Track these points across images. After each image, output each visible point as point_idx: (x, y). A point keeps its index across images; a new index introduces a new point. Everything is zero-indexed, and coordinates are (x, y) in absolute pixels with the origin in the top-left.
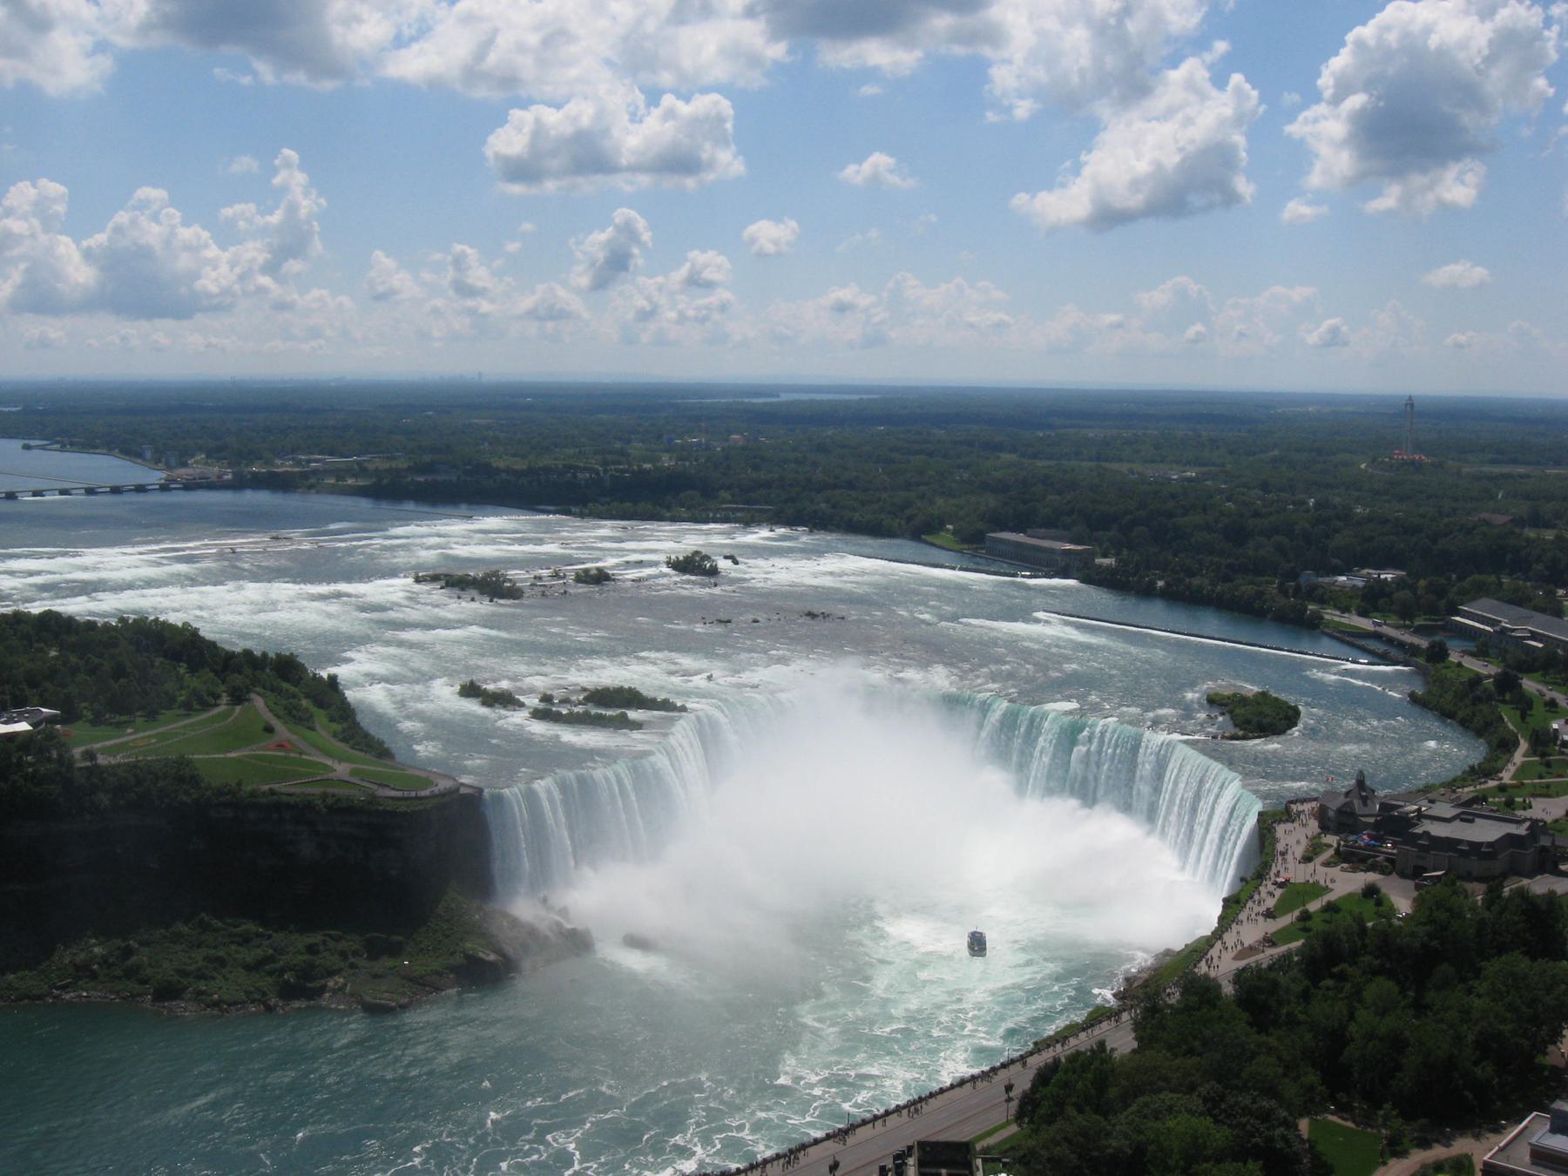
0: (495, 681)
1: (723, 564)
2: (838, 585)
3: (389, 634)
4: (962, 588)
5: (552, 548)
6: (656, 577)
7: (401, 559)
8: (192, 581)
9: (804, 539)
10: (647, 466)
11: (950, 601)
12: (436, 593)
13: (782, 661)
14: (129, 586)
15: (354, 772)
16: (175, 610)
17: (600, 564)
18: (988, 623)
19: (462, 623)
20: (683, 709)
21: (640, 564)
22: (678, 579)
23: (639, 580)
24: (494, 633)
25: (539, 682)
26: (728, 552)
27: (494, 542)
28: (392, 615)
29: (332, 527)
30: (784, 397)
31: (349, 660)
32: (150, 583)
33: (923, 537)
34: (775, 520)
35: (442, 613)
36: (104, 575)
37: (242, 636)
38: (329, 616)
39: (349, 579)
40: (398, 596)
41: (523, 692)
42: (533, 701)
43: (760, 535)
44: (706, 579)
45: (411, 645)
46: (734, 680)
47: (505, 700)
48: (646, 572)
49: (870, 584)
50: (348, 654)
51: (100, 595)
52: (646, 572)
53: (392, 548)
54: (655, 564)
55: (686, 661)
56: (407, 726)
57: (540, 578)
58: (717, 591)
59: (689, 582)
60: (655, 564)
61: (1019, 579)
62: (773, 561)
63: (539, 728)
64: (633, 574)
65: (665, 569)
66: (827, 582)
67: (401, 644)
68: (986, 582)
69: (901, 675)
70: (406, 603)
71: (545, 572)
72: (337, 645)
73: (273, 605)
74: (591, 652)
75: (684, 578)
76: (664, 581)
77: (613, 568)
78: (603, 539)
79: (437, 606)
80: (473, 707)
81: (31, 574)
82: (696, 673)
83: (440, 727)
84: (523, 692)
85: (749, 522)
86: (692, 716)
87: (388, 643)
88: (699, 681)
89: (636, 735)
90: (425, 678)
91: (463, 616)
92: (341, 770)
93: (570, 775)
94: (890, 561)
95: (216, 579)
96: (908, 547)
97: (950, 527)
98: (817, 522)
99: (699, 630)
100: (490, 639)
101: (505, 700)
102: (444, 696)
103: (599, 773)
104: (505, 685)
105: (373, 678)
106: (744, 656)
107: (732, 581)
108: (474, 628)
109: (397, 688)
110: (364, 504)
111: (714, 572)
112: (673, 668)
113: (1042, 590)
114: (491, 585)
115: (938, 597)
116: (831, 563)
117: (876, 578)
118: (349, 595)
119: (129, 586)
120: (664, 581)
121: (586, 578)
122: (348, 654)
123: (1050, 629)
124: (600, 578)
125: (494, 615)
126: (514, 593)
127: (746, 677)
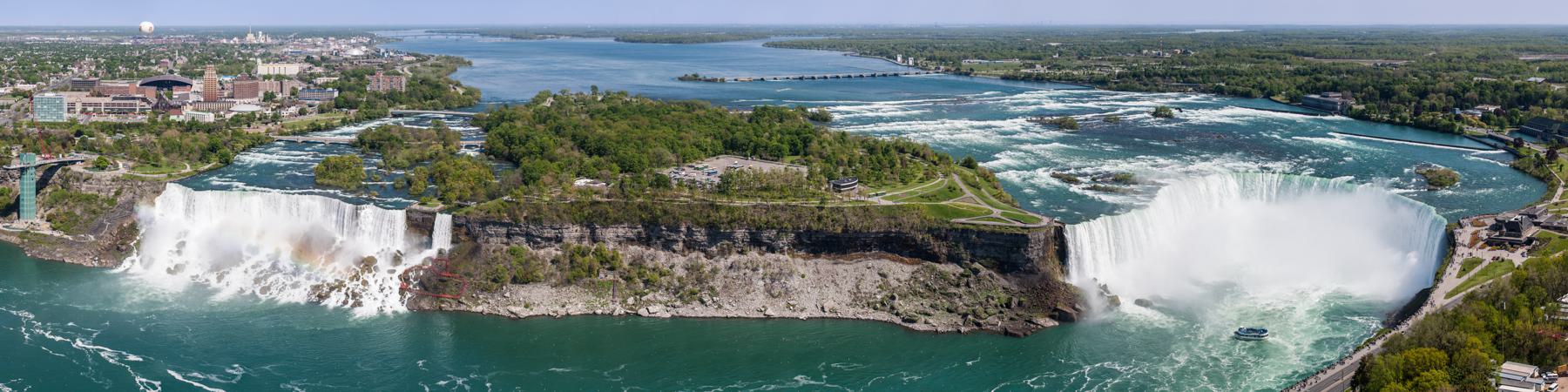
0: (1068, 170)
1: (1175, 112)
2: (1233, 122)
3: (1015, 146)
4: (1293, 122)
5: (1091, 105)
6: (1142, 119)
7: (1020, 109)
8: (922, 118)
9: (1215, 99)
10: (1135, 65)
11: (1286, 129)
12: (1038, 128)
13: (1206, 159)
14: (892, 119)
15: (1003, 214)
16: (916, 132)
17: (1116, 112)
18: (1309, 139)
19: (1051, 142)
20: (1162, 184)
21: (1135, 112)
22: (1153, 119)
23: (1135, 121)
24: (1065, 146)
25: (1089, 170)
26: (1177, 106)
27: (1063, 102)
28: (1015, 137)
29: (986, 93)
30: (1198, 31)
31: (997, 159)
32: (903, 119)
33: (1272, 98)
34: (1198, 90)
35: (1039, 136)
36: (880, 114)
37: (947, 145)
38: (986, 136)
39: (995, 119)
40: (1018, 128)
41: (1080, 175)
42: (1088, 179)
43: (1192, 98)
44: (1167, 119)
45: (1026, 152)
46: (1185, 170)
47: (1071, 180)
48: (1138, 116)
49: (1248, 121)
50: (997, 155)
51: (880, 124)
52: (1138, 116)
53: (1015, 105)
54: (1142, 112)
55: (1161, 161)
56: (1027, 191)
57: (1086, 120)
58: (1173, 125)
59: (1158, 121)
60: (1142, 112)
61: (1319, 117)
62: (1200, 110)
63: (1090, 193)
64: (1131, 117)
65: (1146, 115)
66: (1228, 120)
67: (1021, 151)
68: (1307, 119)
69: (1266, 165)
70: (1021, 130)
71: (1089, 116)
72: (989, 152)
73: (960, 130)
74: (1114, 156)
75: (1157, 119)
76: (1148, 121)
77: (1121, 114)
78: (1116, 100)
79: (1039, 133)
80: (1056, 182)
81: (848, 113)
82: (1167, 166)
83: (1043, 193)
84: (1080, 175)
85: (1185, 92)
86: (1166, 188)
87: (1015, 150)
88: (1166, 170)
89: (1138, 197)
90: (1035, 168)
91: (1050, 138)
92: (997, 212)
93: (1109, 218)
94: (1257, 109)
95: (933, 117)
96: (1264, 103)
97: (1284, 93)
98: (1219, 92)
99: (1166, 145)
100: (1063, 149)
101: (1071, 180)
102: (1043, 177)
103: (1123, 218)
104: (1072, 171)
105: (1009, 168)
106: (1188, 158)
107: (1178, 120)
108: (1056, 144)
109: (1021, 172)
110: (1002, 83)
111: (1170, 117)
112: (1154, 163)
113: (1331, 122)
114: (1061, 122)
115: (1282, 127)
116: (1228, 111)
117: (1252, 118)
118: (994, 127)
119: (892, 119)
120: (1148, 121)
121: (1107, 119)
122: (997, 155)
123: (1338, 141)
124: (1115, 120)
125: (1064, 137)
126: (1072, 126)
127: (1191, 168)
